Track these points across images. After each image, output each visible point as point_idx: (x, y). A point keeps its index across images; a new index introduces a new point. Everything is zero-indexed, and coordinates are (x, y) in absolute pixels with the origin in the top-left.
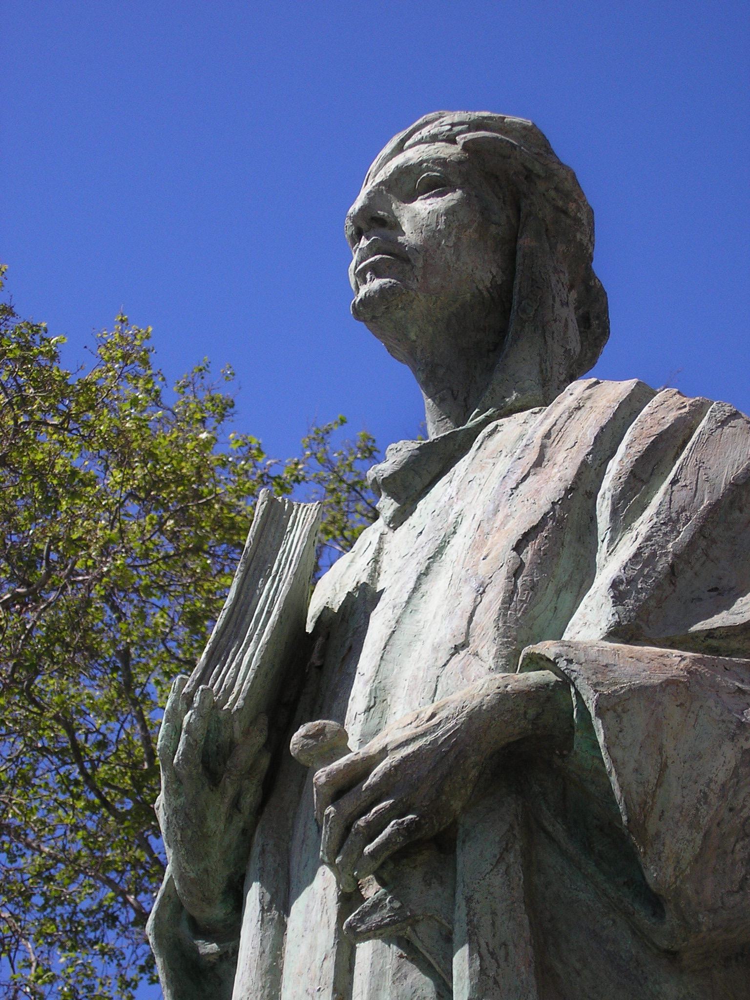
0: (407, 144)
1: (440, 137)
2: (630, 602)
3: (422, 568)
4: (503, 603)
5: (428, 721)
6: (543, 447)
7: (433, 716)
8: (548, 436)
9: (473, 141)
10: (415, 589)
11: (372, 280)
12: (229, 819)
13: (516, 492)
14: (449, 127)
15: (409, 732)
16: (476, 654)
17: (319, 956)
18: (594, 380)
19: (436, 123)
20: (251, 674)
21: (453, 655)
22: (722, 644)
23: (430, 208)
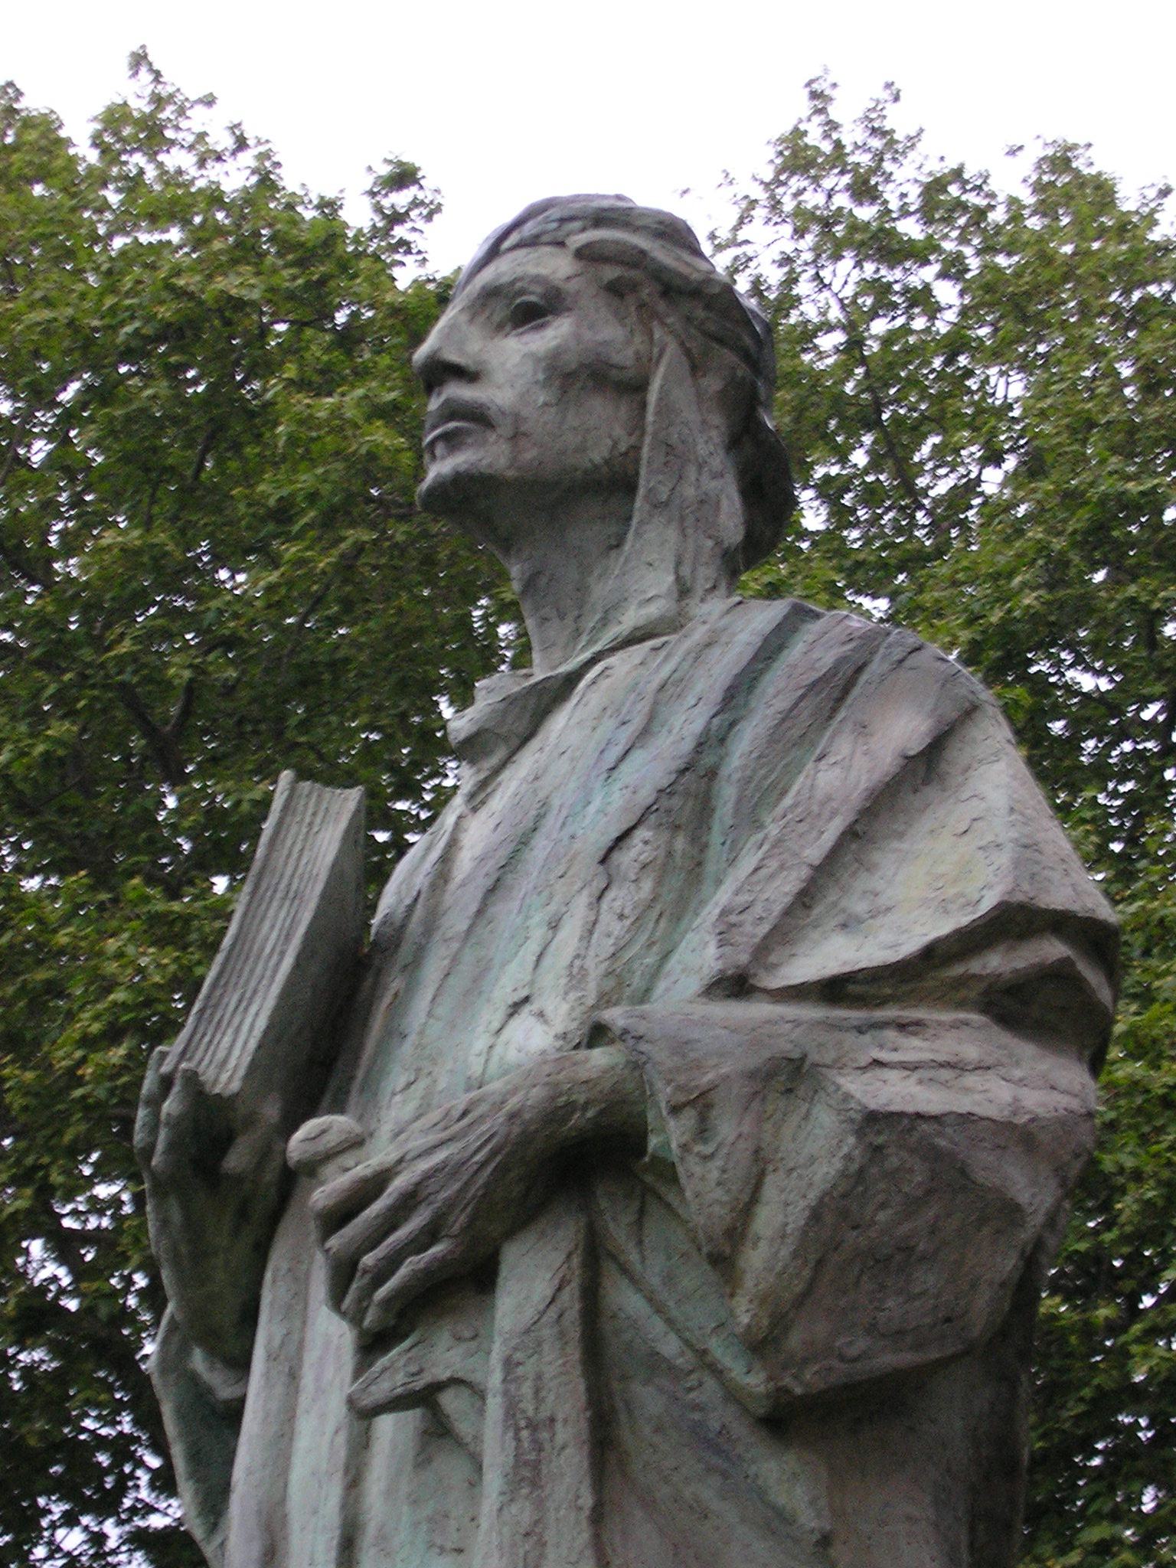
0: (506, 244)
1: (545, 238)
2: (600, 1058)
3: (489, 882)
4: (581, 939)
5: (459, 1120)
6: (656, 703)
7: (465, 1114)
8: (662, 687)
9: (588, 245)
10: (480, 912)
11: (443, 458)
12: (236, 1231)
13: (615, 774)
14: (554, 225)
15: (433, 1138)
16: (541, 1015)
17: (330, 1428)
18: (738, 599)
19: (541, 217)
20: (253, 1044)
21: (511, 1015)
22: (872, 990)
23: (525, 349)
